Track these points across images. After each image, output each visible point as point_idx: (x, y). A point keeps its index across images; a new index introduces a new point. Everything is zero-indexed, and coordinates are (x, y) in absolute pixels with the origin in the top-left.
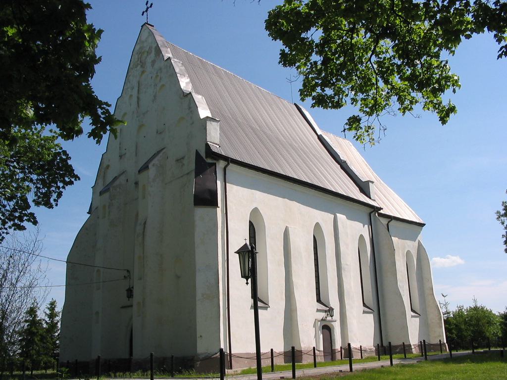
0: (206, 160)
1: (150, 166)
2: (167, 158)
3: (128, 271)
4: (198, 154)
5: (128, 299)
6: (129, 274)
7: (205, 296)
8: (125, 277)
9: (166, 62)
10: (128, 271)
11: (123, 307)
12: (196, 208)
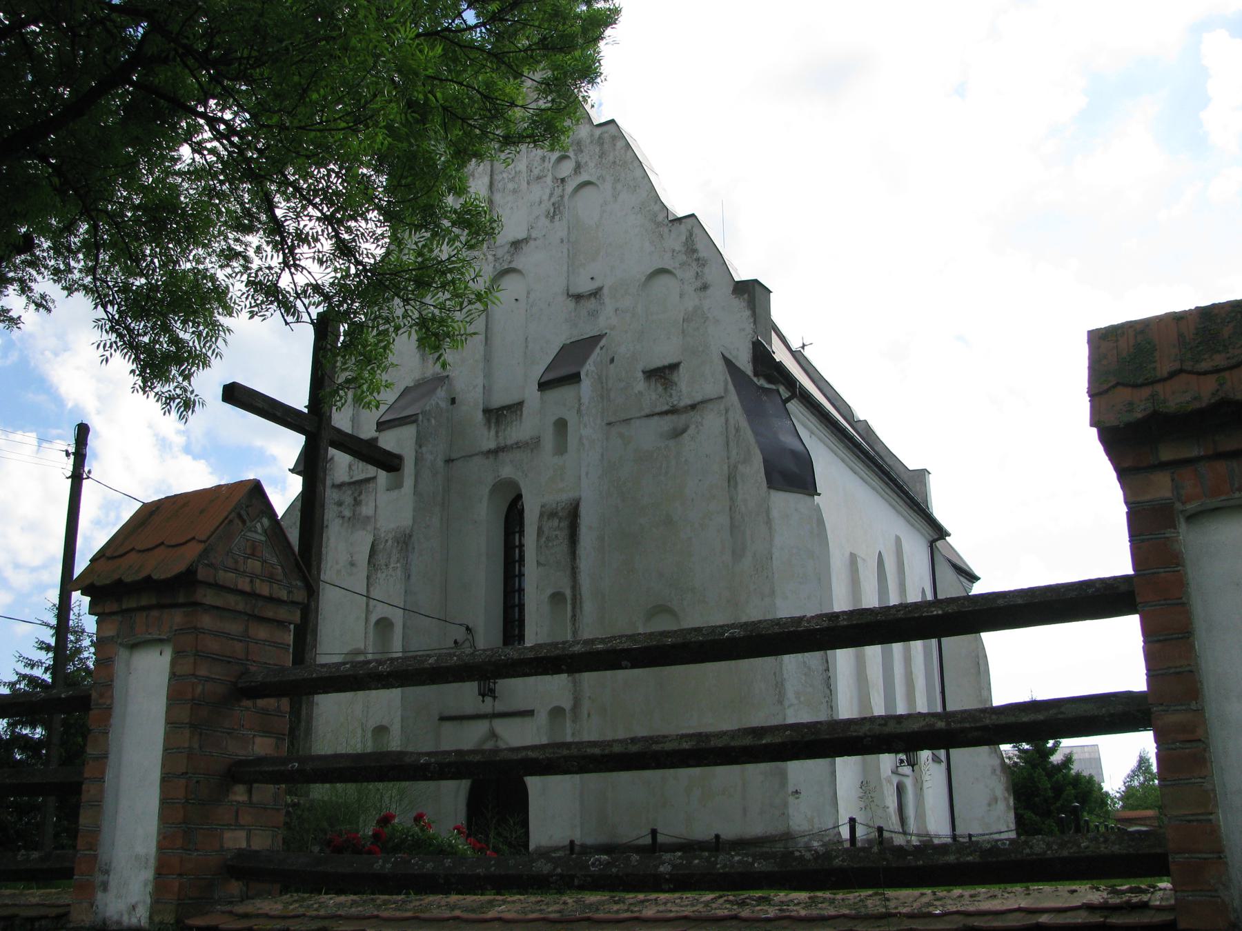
0: (755, 379)
1: (583, 376)
2: (612, 360)
3: (468, 629)
4: (729, 364)
5: (481, 698)
6: (470, 637)
7: (802, 699)
8: (456, 642)
9: (598, 132)
10: (468, 629)
11: (443, 719)
12: (773, 493)
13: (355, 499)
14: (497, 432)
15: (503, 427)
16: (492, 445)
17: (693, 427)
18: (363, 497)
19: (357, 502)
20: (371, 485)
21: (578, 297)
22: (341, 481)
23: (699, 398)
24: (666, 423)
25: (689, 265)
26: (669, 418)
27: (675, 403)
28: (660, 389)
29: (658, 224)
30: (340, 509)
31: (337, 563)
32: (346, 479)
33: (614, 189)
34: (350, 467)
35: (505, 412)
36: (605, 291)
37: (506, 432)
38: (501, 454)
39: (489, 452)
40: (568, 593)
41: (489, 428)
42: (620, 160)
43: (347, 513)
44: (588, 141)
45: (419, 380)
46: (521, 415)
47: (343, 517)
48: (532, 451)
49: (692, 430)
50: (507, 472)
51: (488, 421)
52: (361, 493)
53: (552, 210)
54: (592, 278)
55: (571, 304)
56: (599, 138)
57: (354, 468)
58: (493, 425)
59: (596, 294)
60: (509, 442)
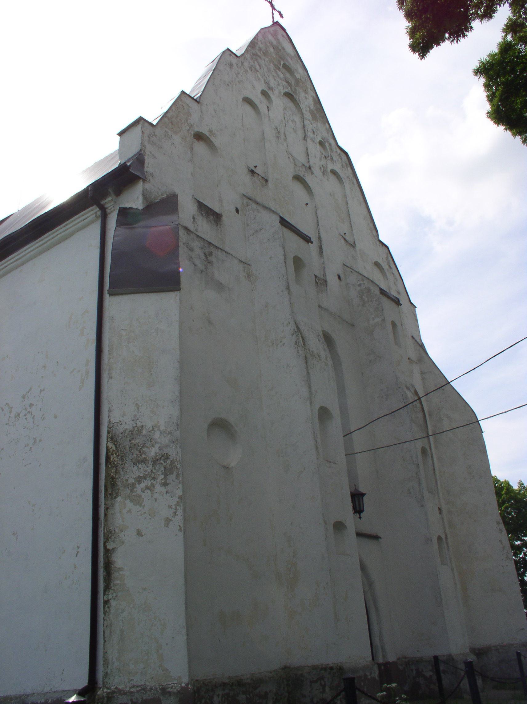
29: (374, 236)
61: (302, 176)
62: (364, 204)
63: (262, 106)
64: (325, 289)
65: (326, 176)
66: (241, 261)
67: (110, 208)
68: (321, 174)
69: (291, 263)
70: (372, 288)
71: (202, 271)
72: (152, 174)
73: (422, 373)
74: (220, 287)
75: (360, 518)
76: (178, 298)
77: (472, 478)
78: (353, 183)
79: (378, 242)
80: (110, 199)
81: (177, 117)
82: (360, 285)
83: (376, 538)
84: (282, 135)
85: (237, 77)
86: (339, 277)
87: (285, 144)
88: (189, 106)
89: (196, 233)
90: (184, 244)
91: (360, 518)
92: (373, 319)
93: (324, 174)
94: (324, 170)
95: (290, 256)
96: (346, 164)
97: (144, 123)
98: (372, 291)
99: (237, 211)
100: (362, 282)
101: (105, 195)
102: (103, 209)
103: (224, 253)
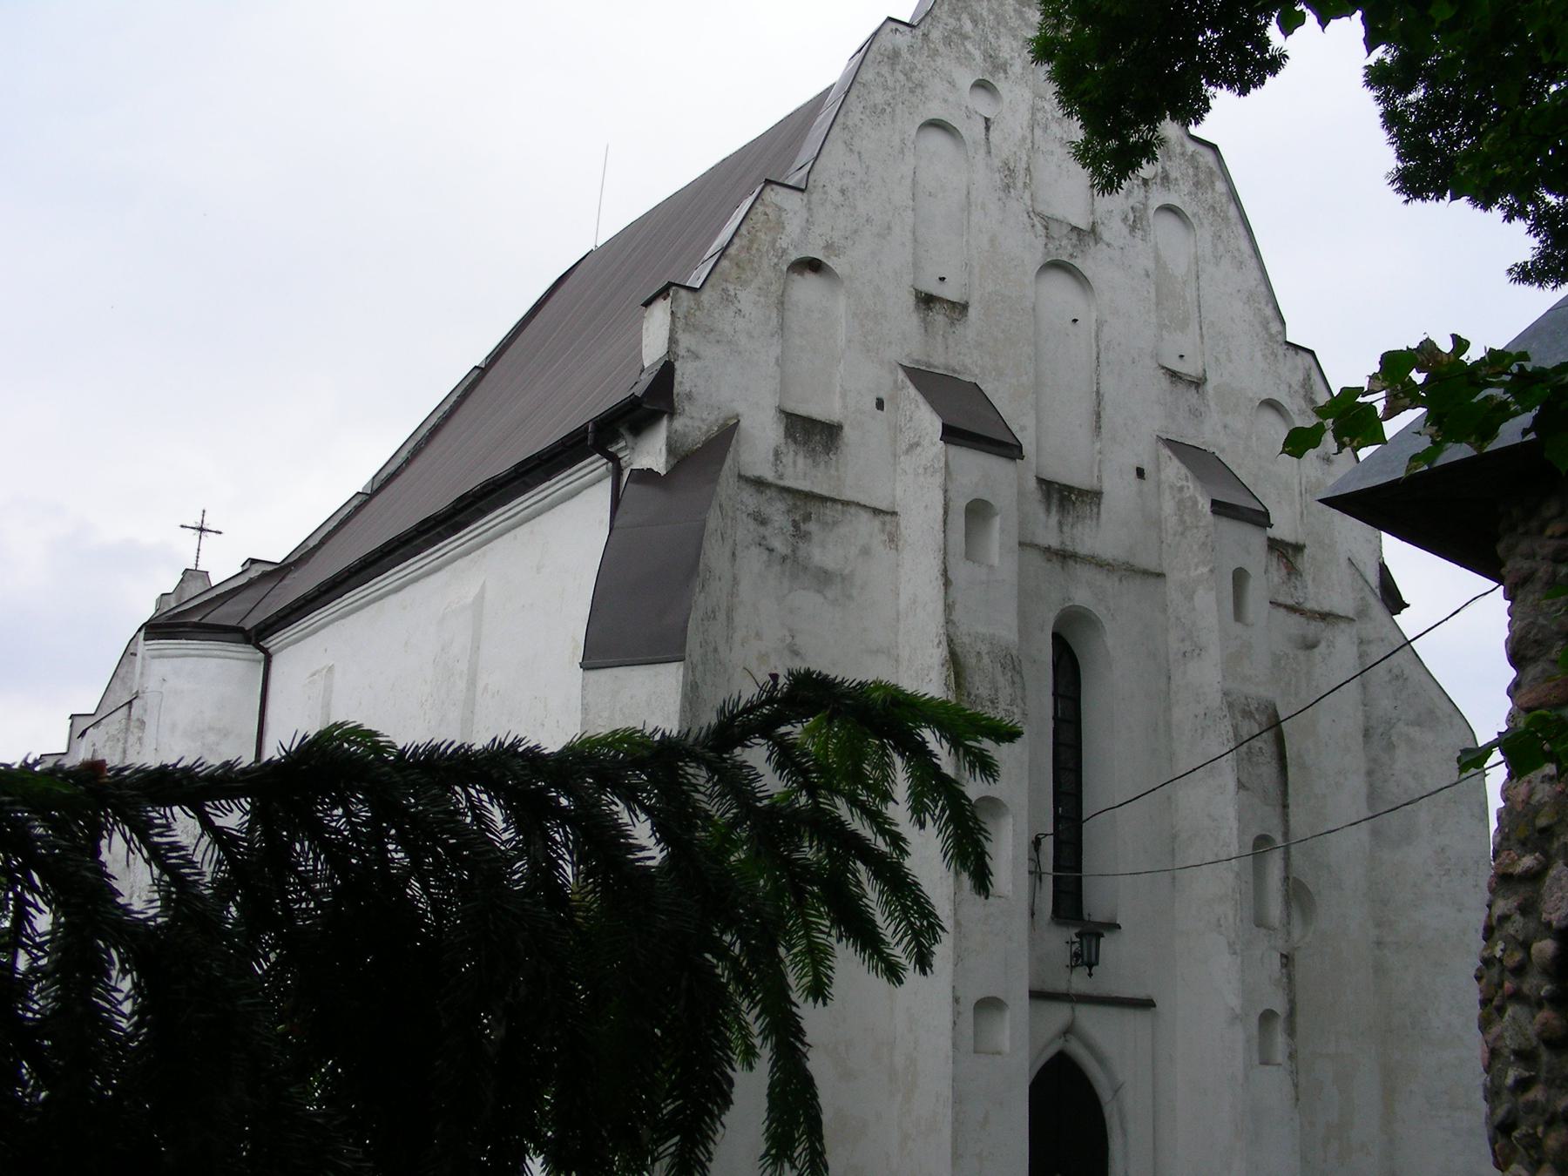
13: (795, 524)
14: (1060, 524)
15: (1070, 519)
16: (1053, 541)
17: (1323, 645)
18: (812, 527)
19: (799, 533)
20: (828, 511)
21: (1174, 375)
22: (757, 473)
23: (1326, 608)
24: (1294, 623)
25: (1309, 417)
26: (1296, 618)
27: (1301, 600)
28: (1284, 571)
29: (1271, 336)
30: (762, 530)
31: (758, 636)
32: (769, 475)
33: (1215, 246)
34: (777, 454)
35: (1073, 497)
36: (1209, 387)
37: (1075, 531)
38: (1071, 562)
39: (1048, 551)
40: (1279, 839)
41: (1048, 510)
42: (1221, 211)
43: (778, 544)
44: (1178, 150)
45: (918, 362)
46: (1098, 513)
47: (771, 550)
48: (1120, 580)
49: (1322, 647)
50: (1082, 597)
51: (1047, 497)
52: (807, 518)
53: (1131, 217)
54: (1182, 356)
55: (1165, 382)
56: (1192, 155)
57: (788, 460)
58: (1054, 509)
59: (1198, 383)
60: (1082, 550)
61: (1065, 258)
62: (1253, 263)
63: (972, 131)
64: (1095, 510)
65: (1139, 233)
66: (877, 511)
67: (625, 459)
68: (1125, 231)
69: (958, 521)
70: (1199, 498)
71: (784, 558)
72: (689, 396)
73: (1361, 642)
74: (824, 578)
75: (1090, 975)
76: (682, 669)
77: (1444, 875)
78: (1226, 219)
79: (1281, 350)
80: (622, 444)
81: (749, 249)
82: (1181, 489)
83: (1147, 1004)
84: (1021, 174)
85: (909, 79)
86: (1140, 473)
87: (1027, 196)
88: (780, 209)
89: (781, 483)
90: (749, 514)
91: (1090, 975)
92: (1197, 566)
93: (1133, 228)
94: (1135, 216)
95: (960, 505)
96: (1211, 173)
97: (676, 293)
98: (1200, 506)
99: (880, 404)
100: (1184, 483)
101: (616, 437)
102: (614, 458)
103: (840, 507)
